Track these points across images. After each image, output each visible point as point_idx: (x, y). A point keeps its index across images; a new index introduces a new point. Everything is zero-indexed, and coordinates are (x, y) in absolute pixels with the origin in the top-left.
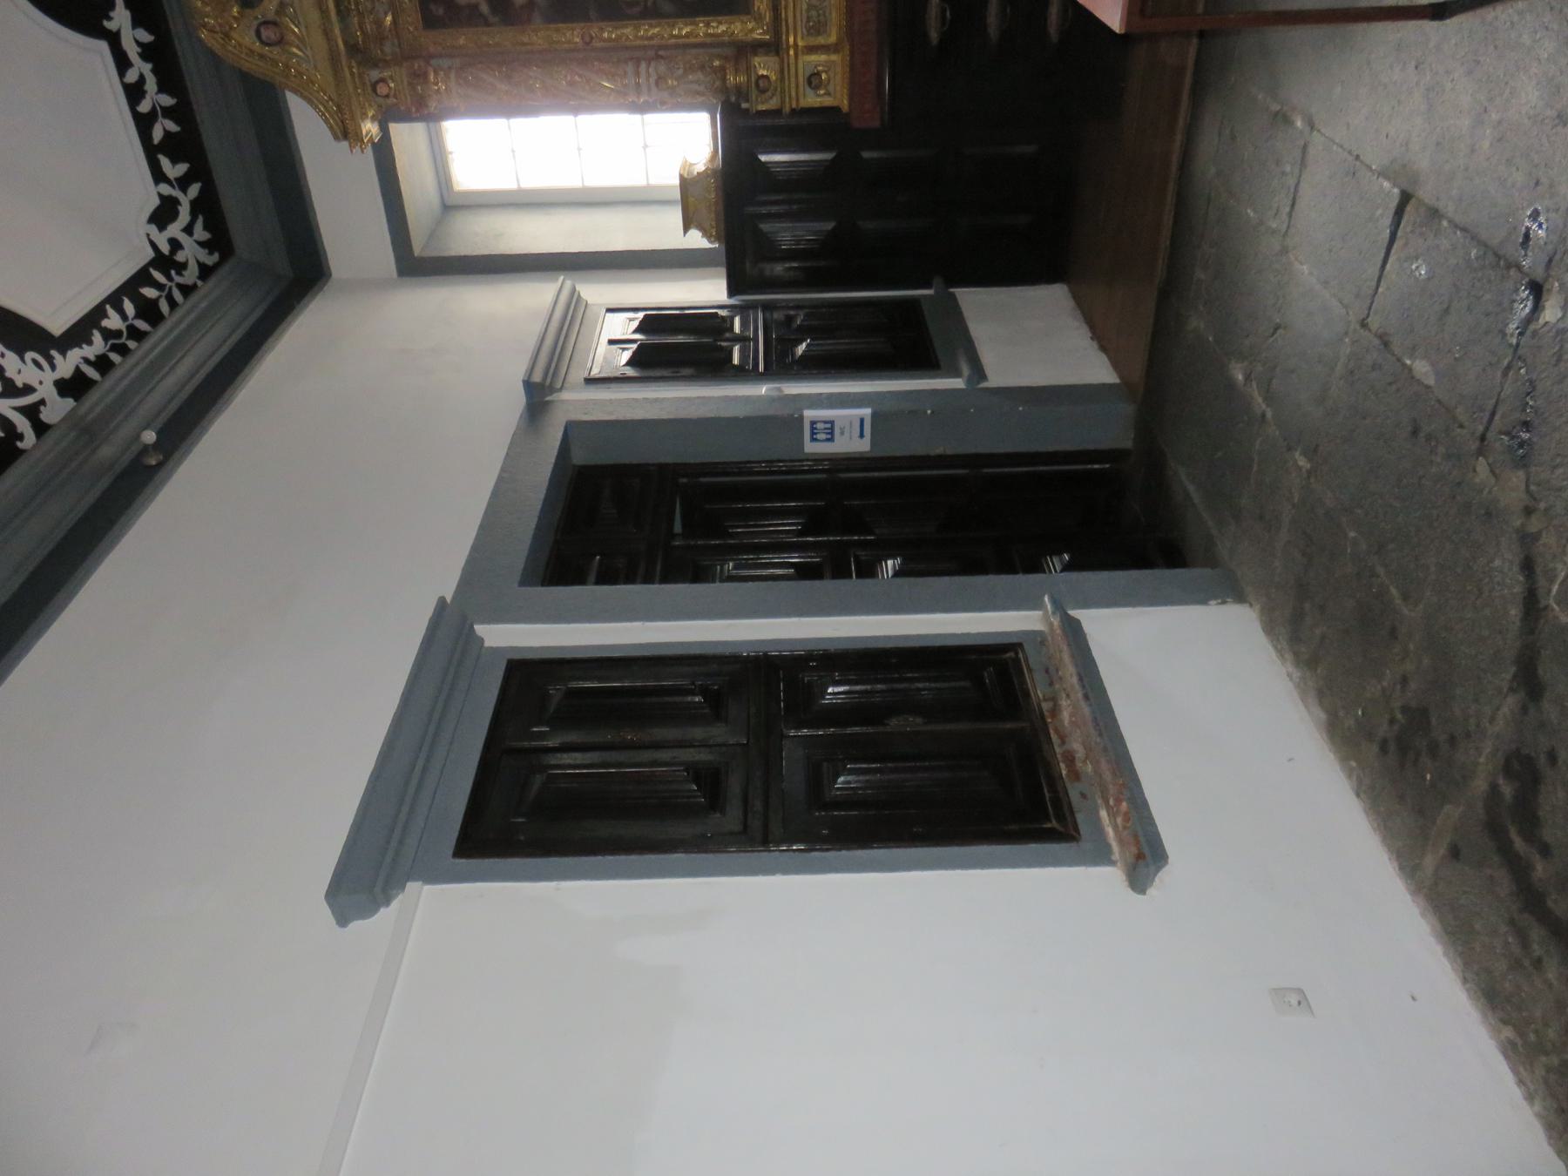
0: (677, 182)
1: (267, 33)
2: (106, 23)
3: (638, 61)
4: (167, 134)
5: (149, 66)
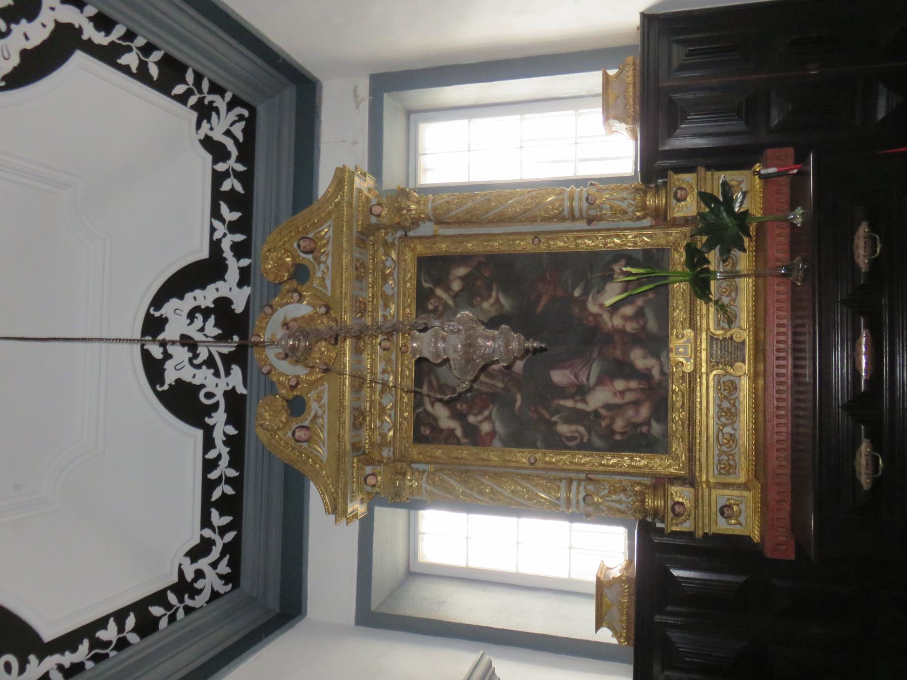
0: (594, 579)
1: (300, 434)
2: (207, 420)
3: (570, 481)
4: (224, 494)
5: (228, 449)
